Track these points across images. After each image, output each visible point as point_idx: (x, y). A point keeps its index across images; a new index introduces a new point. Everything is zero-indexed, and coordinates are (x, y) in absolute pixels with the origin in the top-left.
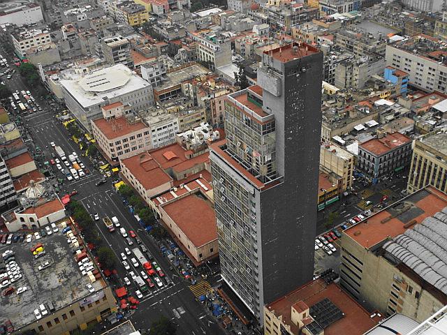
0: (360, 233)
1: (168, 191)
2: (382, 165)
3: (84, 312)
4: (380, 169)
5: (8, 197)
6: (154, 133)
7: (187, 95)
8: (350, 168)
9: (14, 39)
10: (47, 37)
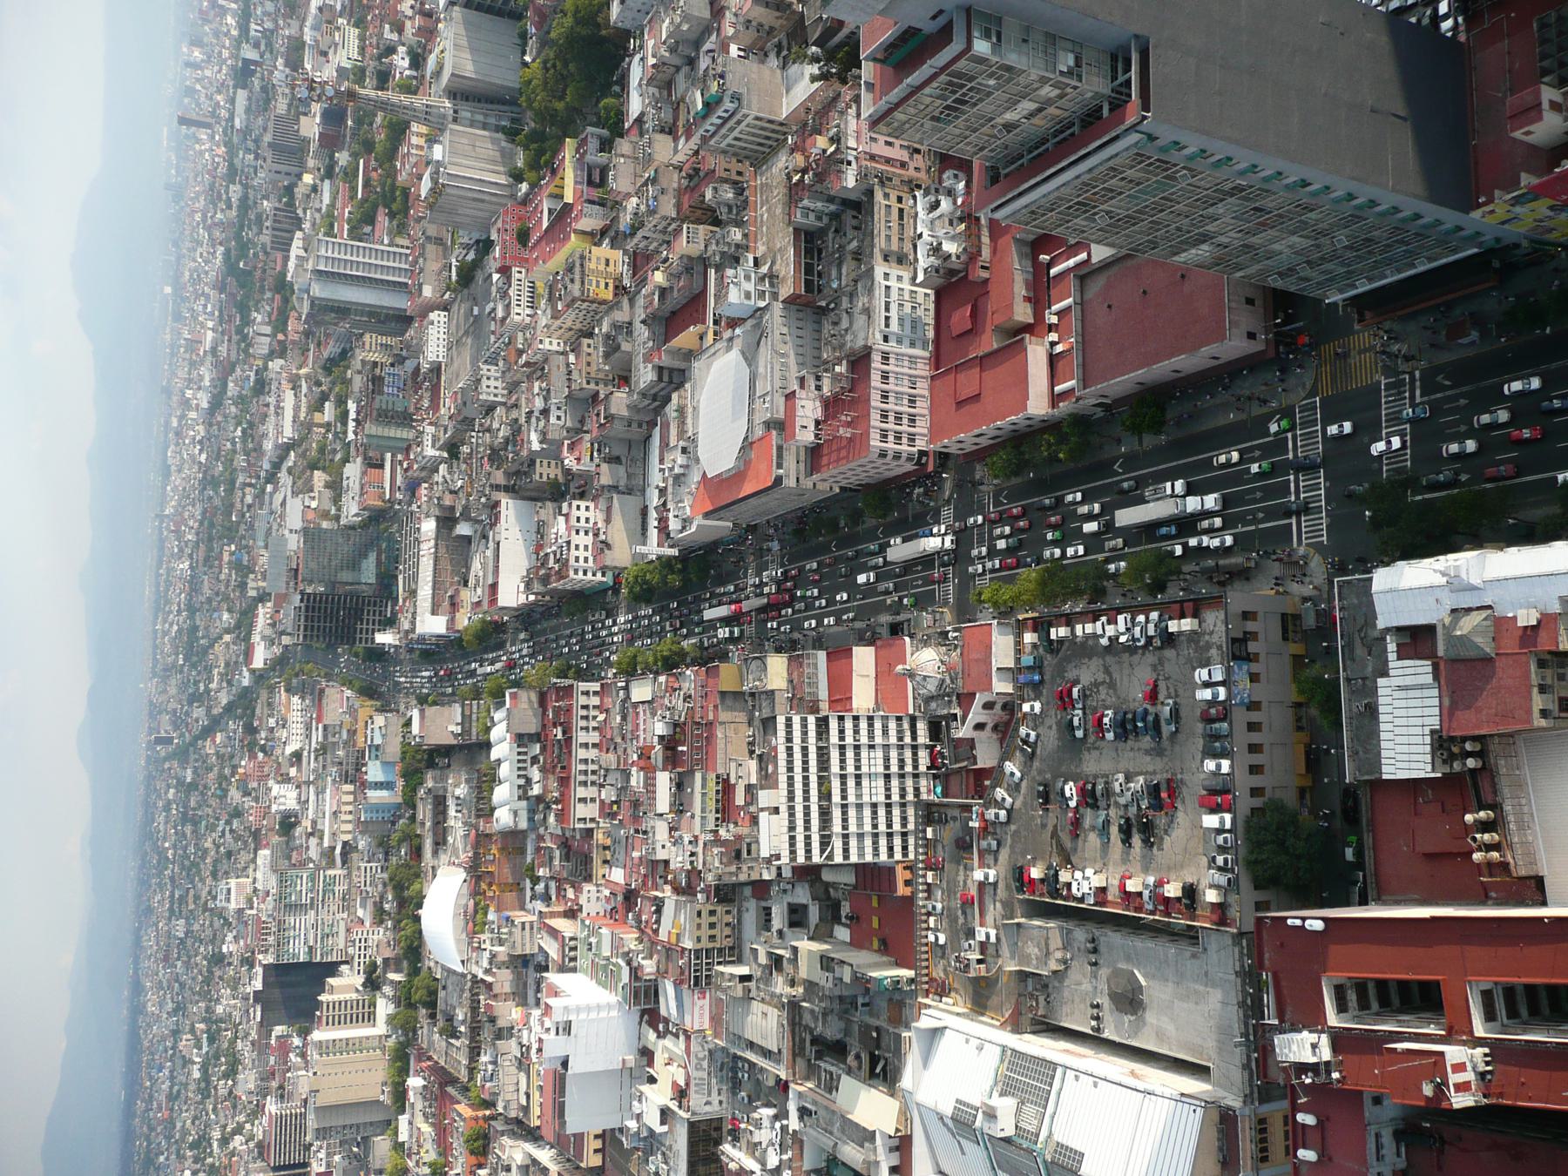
7: (826, 220)
10: (578, 508)
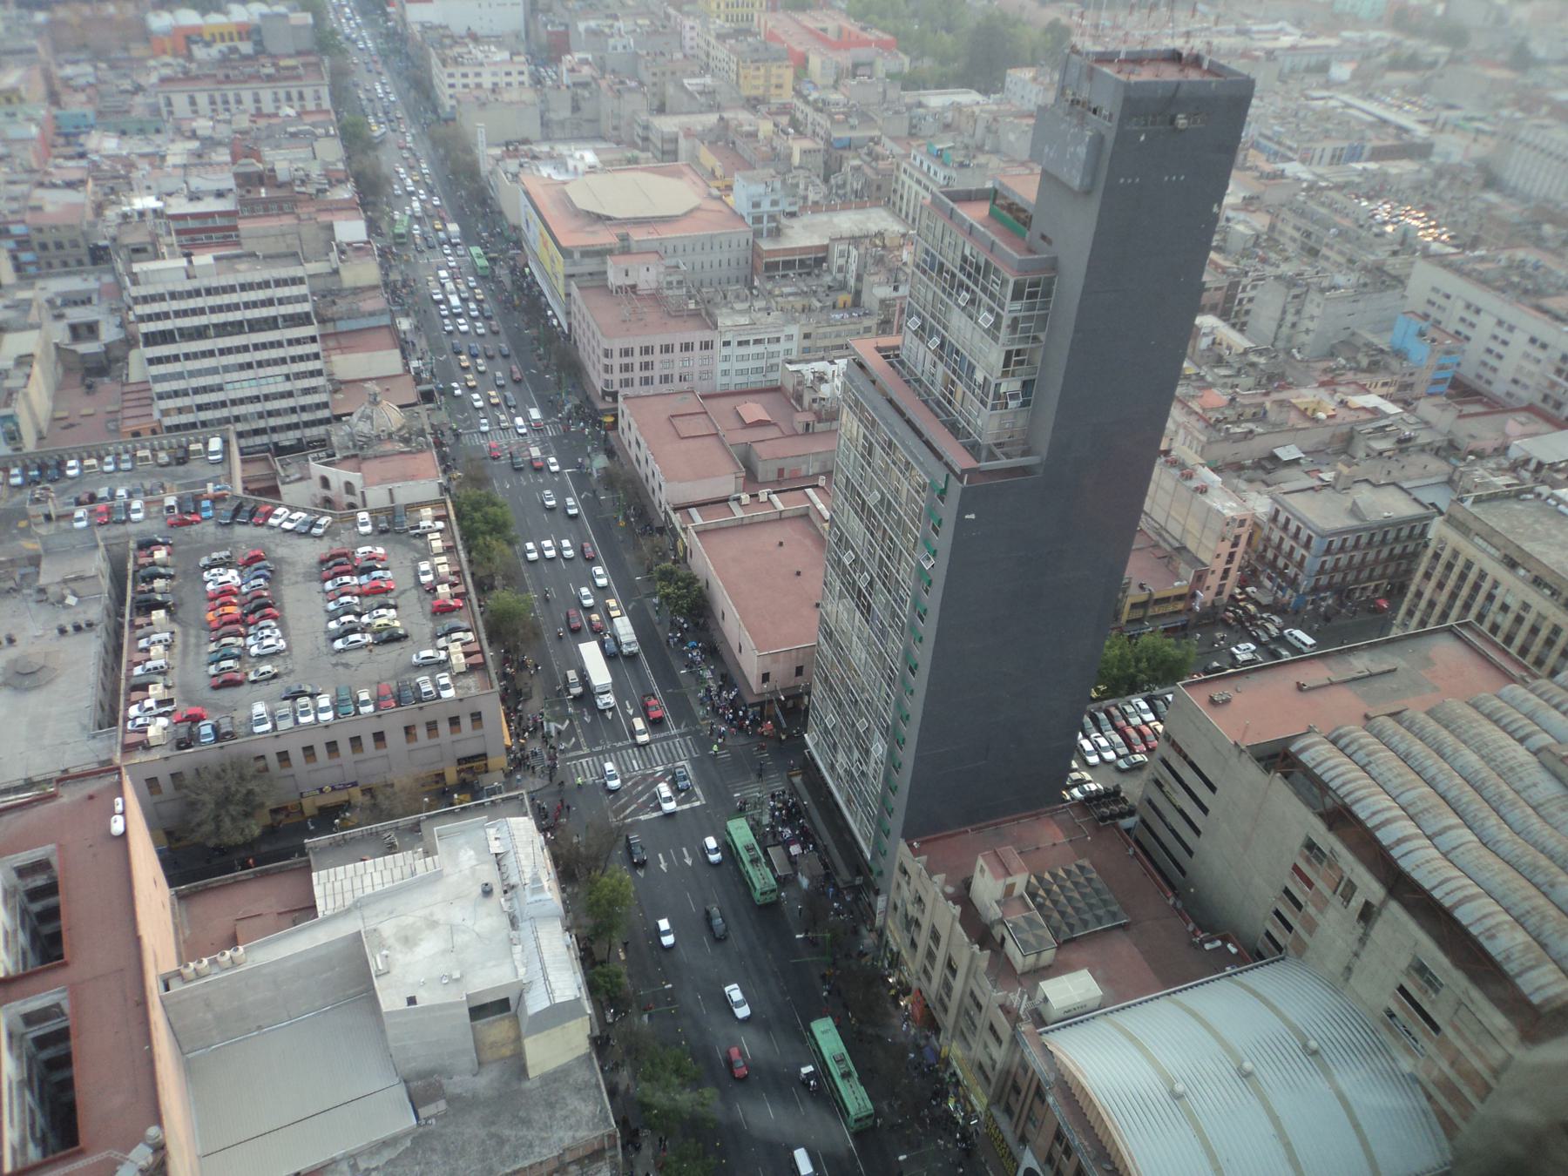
0: (1227, 701)
1: (725, 500)
2: (1330, 561)
3: (414, 745)
4: (1322, 571)
5: (307, 424)
6: (726, 351)
7: (840, 276)
8: (1235, 545)
9: (435, 61)
10: (521, 73)
